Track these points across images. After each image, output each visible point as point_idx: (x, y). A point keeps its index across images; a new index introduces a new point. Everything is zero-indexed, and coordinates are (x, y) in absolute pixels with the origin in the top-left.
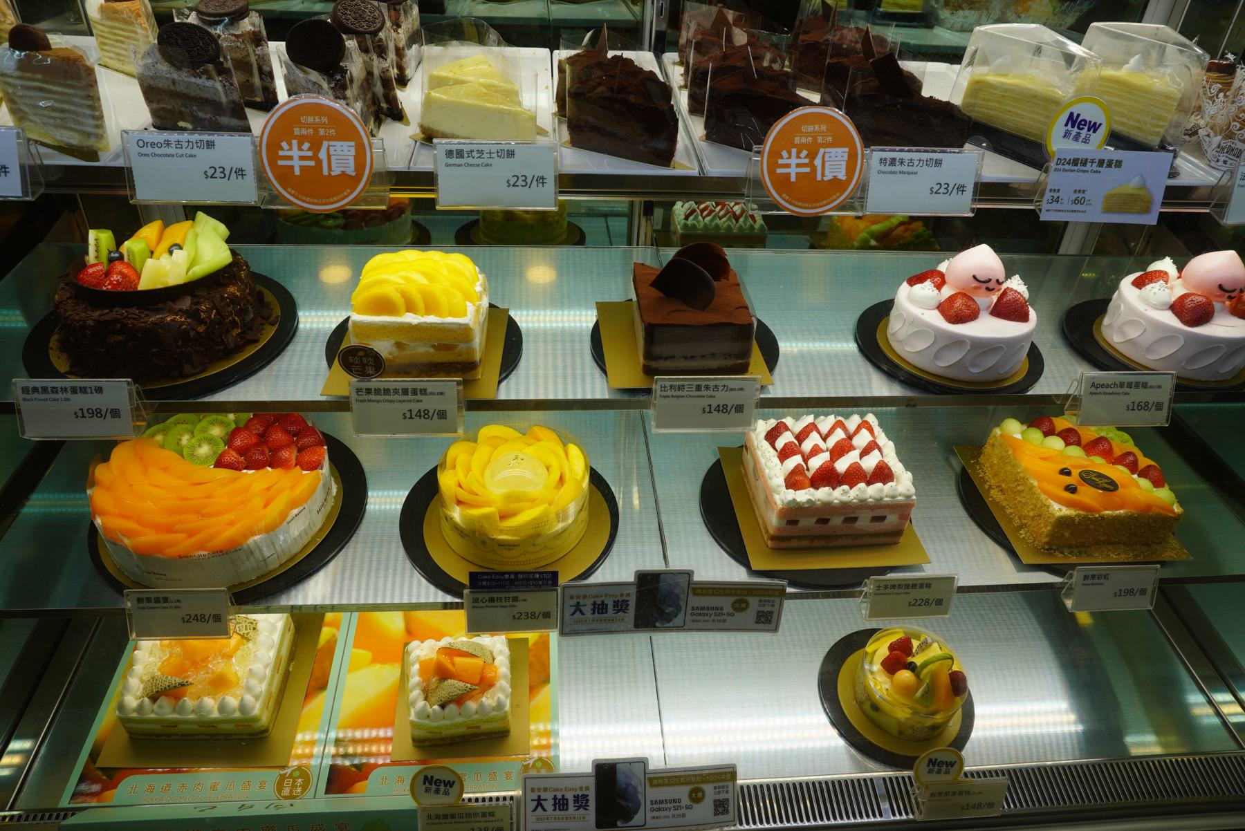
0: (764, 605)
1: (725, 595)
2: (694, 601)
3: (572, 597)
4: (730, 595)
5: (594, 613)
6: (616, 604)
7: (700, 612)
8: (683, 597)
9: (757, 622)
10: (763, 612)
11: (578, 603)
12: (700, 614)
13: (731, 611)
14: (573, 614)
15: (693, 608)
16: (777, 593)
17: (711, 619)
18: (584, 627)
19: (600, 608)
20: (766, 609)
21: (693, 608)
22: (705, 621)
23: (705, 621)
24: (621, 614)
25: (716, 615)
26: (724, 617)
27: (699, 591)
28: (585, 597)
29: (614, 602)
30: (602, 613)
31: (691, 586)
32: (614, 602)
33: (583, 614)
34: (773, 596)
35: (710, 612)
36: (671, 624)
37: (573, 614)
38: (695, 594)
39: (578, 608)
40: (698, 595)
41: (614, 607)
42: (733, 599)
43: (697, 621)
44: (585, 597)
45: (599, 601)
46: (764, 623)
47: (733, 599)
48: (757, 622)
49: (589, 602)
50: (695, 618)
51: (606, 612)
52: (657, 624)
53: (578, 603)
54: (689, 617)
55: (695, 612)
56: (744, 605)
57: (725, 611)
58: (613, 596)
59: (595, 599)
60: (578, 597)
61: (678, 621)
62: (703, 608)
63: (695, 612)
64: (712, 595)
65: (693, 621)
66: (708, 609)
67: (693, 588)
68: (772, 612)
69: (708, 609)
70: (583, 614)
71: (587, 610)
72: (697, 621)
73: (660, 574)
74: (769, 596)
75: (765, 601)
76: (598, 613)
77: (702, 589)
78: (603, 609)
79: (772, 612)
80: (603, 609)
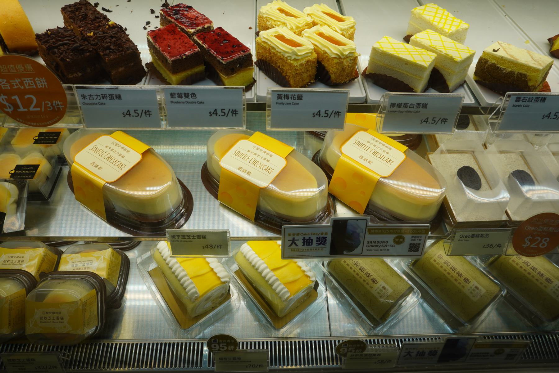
0: (414, 240)
1: (389, 233)
2: (369, 237)
3: (290, 235)
4: (392, 233)
5: (304, 245)
6: (319, 239)
7: (372, 244)
8: (362, 235)
9: (409, 251)
10: (414, 244)
11: (294, 238)
12: (372, 246)
13: (393, 243)
14: (290, 246)
15: (368, 242)
16: (424, 231)
17: (379, 249)
18: (298, 253)
19: (308, 242)
20: (415, 242)
21: (368, 242)
22: (375, 250)
23: (375, 250)
24: (321, 246)
25: (383, 246)
26: (388, 248)
27: (373, 231)
28: (298, 234)
29: (317, 238)
30: (309, 245)
31: (367, 228)
32: (317, 238)
33: (297, 245)
34: (421, 233)
35: (379, 244)
36: (351, 253)
37: (290, 246)
38: (370, 233)
39: (293, 242)
40: (372, 233)
41: (317, 241)
42: (394, 236)
43: (370, 250)
44: (298, 234)
45: (307, 237)
46: (414, 251)
47: (394, 236)
48: (409, 251)
49: (300, 238)
50: (369, 248)
51: (312, 245)
52: (345, 252)
53: (294, 238)
54: (365, 248)
55: (370, 244)
56: (401, 240)
57: (389, 244)
58: (316, 234)
59: (304, 236)
60: (294, 235)
61: (358, 250)
62: (374, 242)
63: (370, 244)
64: (382, 233)
65: (368, 250)
66: (378, 242)
67: (368, 229)
68: (419, 244)
69: (378, 243)
70: (297, 245)
71: (300, 243)
72: (370, 250)
73: (348, 220)
74: (418, 233)
75: (415, 237)
76: (307, 245)
77: (374, 229)
78: (309, 242)
79: (419, 244)
80: (309, 242)
